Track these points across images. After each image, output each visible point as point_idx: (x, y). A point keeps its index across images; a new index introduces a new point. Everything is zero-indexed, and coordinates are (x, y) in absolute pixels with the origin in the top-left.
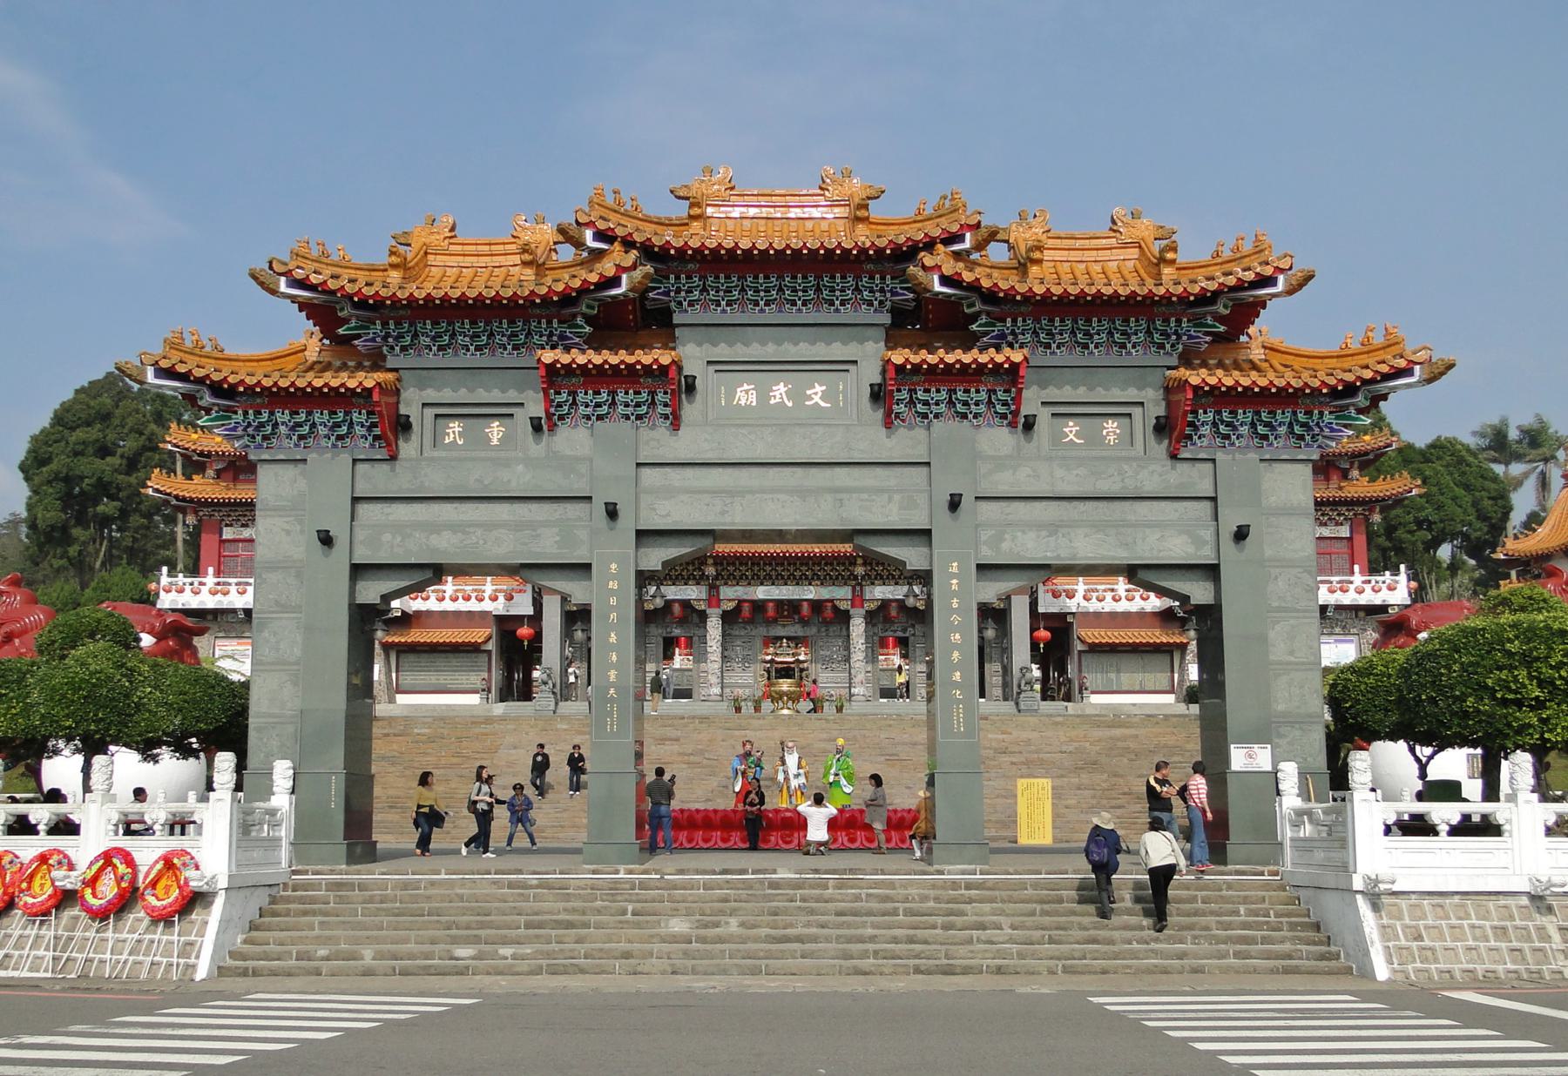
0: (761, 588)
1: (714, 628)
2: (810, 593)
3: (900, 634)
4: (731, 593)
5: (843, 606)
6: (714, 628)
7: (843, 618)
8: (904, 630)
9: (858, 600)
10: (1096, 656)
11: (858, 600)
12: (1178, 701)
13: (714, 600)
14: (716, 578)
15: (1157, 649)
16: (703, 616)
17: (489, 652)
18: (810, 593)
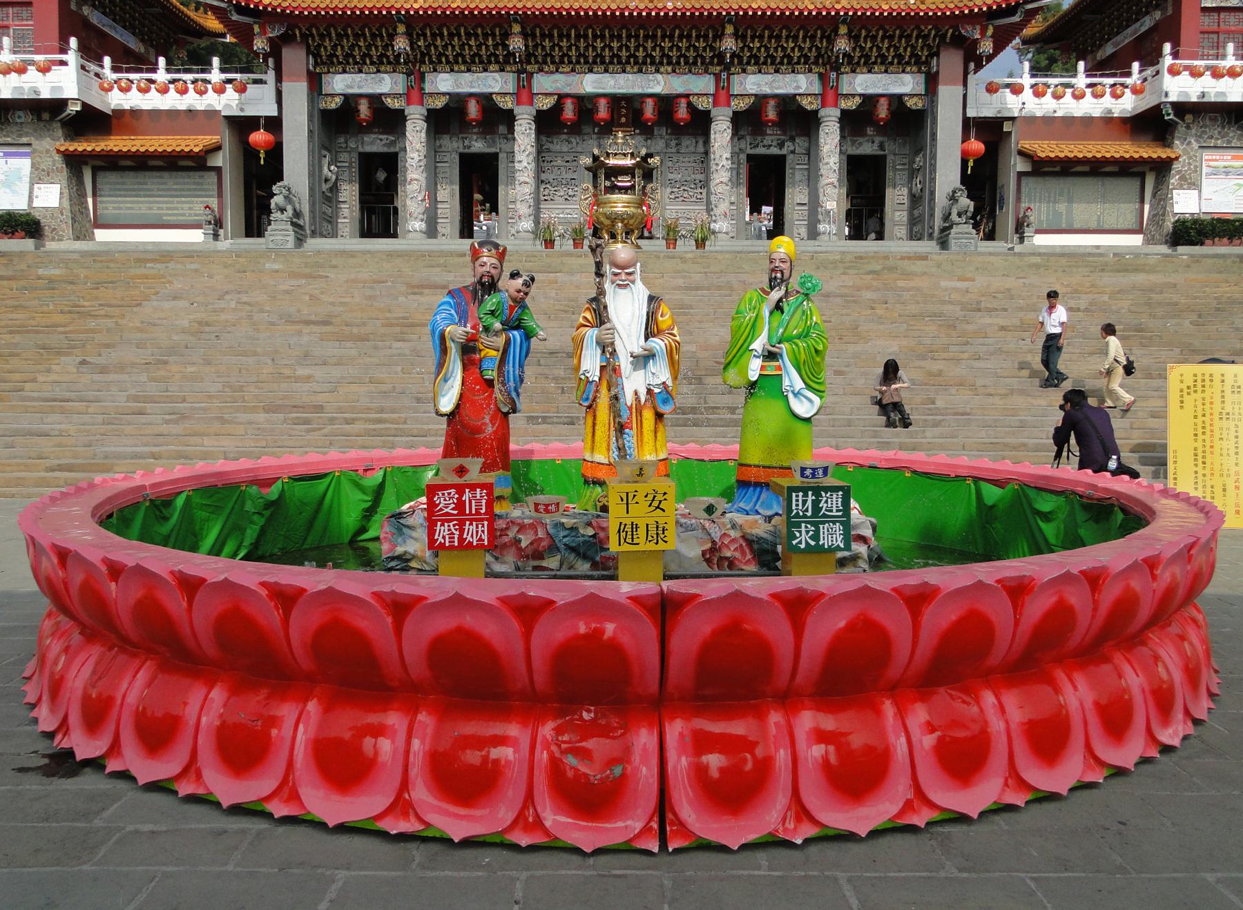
0: (589, 78)
1: (525, 135)
2: (657, 84)
3: (775, 151)
4: (549, 84)
5: (703, 104)
6: (525, 135)
7: (700, 123)
8: (781, 145)
9: (722, 94)
10: (1040, 179)
11: (722, 94)
12: (1147, 242)
13: (524, 93)
14: (529, 57)
15: (1126, 169)
16: (509, 118)
17: (218, 170)
18: (657, 84)
